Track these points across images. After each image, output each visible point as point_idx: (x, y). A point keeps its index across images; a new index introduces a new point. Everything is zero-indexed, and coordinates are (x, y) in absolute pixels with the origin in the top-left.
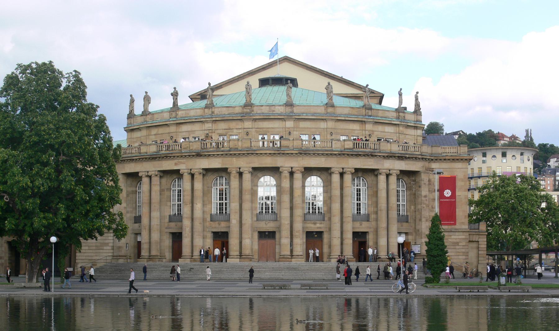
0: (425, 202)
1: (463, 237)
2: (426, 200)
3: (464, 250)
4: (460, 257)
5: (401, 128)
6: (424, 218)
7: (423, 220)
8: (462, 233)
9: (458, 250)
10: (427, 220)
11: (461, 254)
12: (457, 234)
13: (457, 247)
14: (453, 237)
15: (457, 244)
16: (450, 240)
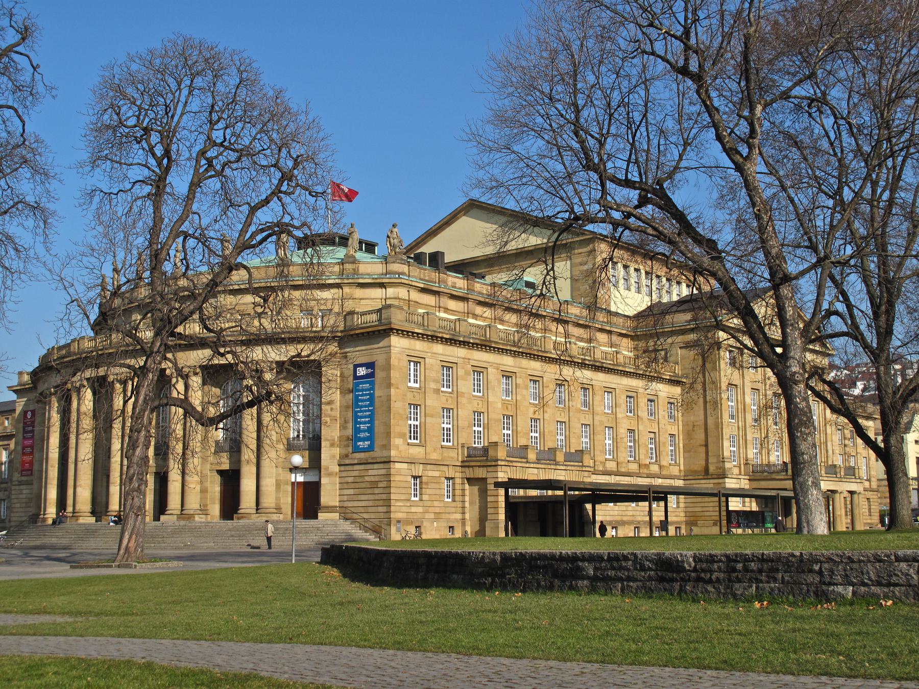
0: (329, 412)
1: (383, 472)
2: (332, 409)
3: (384, 497)
4: (381, 509)
5: (347, 290)
6: (327, 440)
7: (323, 444)
8: (381, 466)
9: (377, 497)
10: (332, 445)
11: (381, 503)
12: (376, 466)
13: (376, 491)
14: (371, 472)
15: (374, 485)
16: (367, 478)
